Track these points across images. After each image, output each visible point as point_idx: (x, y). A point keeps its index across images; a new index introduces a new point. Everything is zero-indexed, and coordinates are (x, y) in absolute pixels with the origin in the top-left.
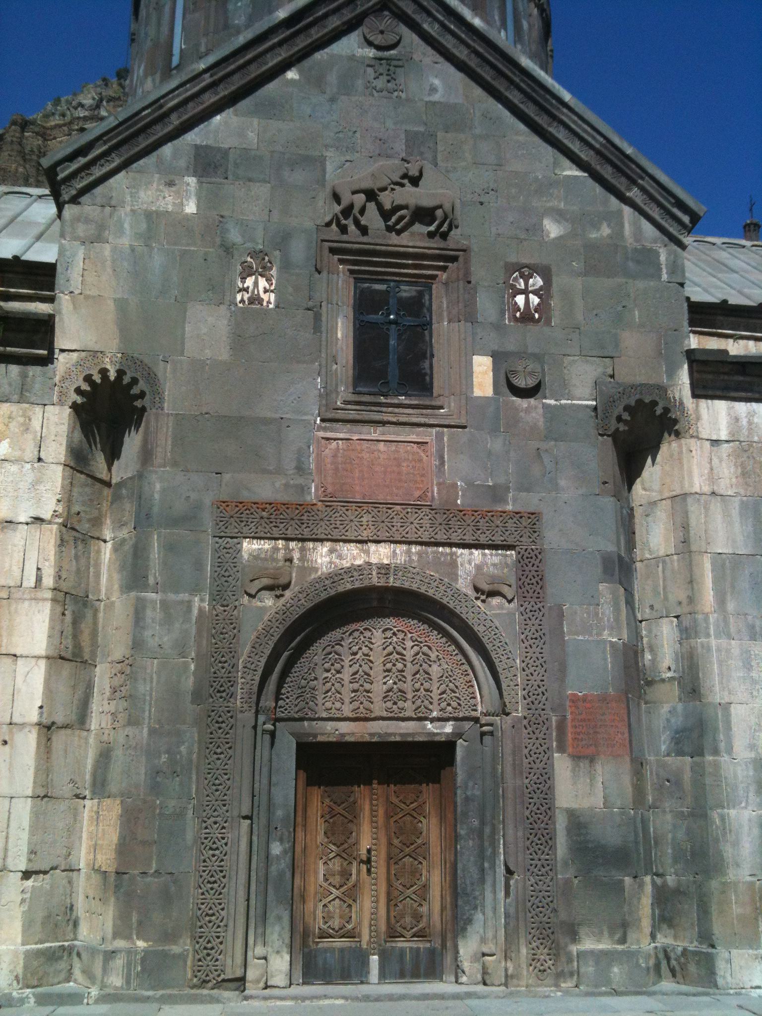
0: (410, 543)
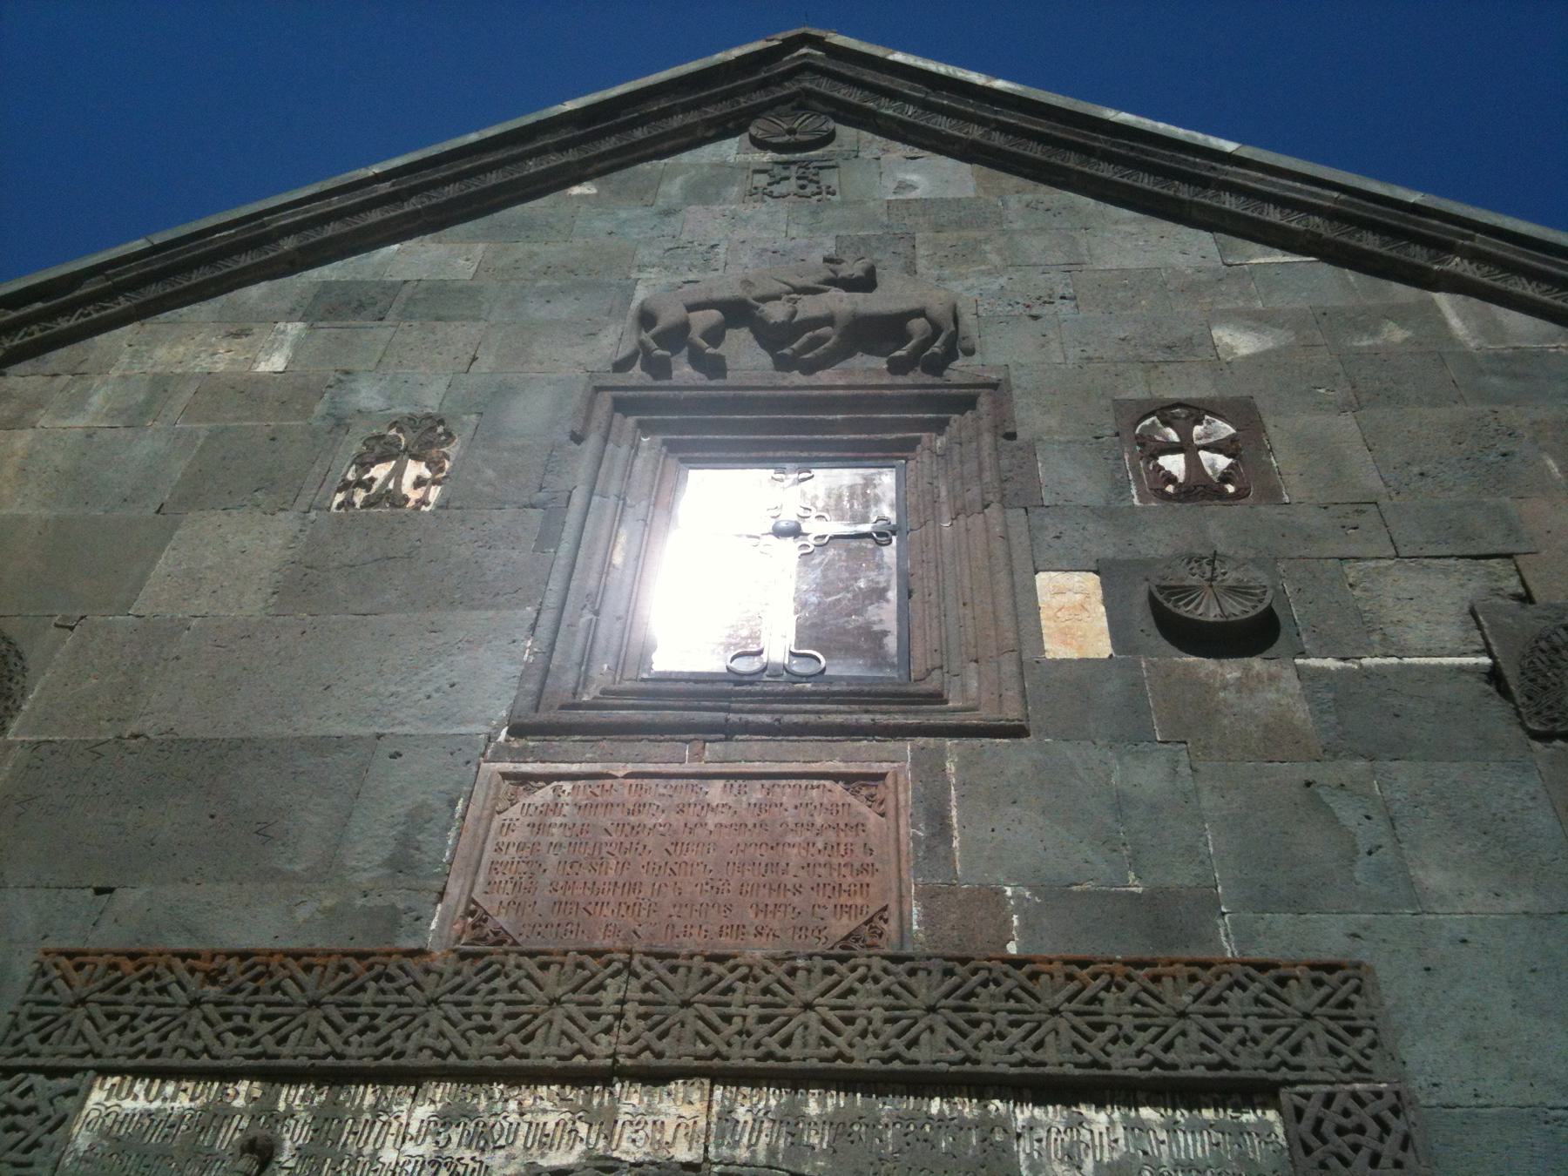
0: (797, 1080)
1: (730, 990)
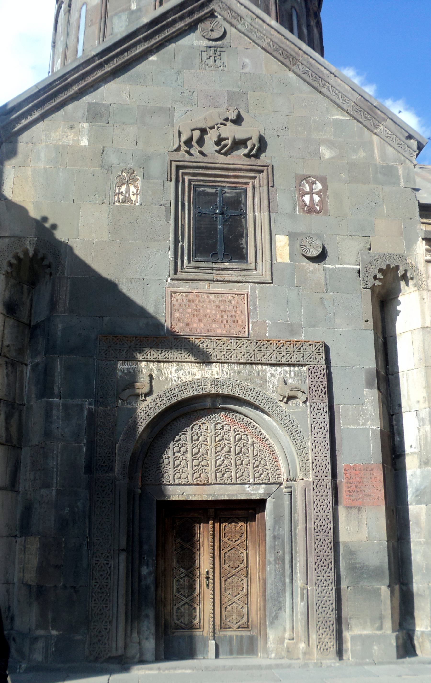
0: (233, 363)
1: (221, 346)
